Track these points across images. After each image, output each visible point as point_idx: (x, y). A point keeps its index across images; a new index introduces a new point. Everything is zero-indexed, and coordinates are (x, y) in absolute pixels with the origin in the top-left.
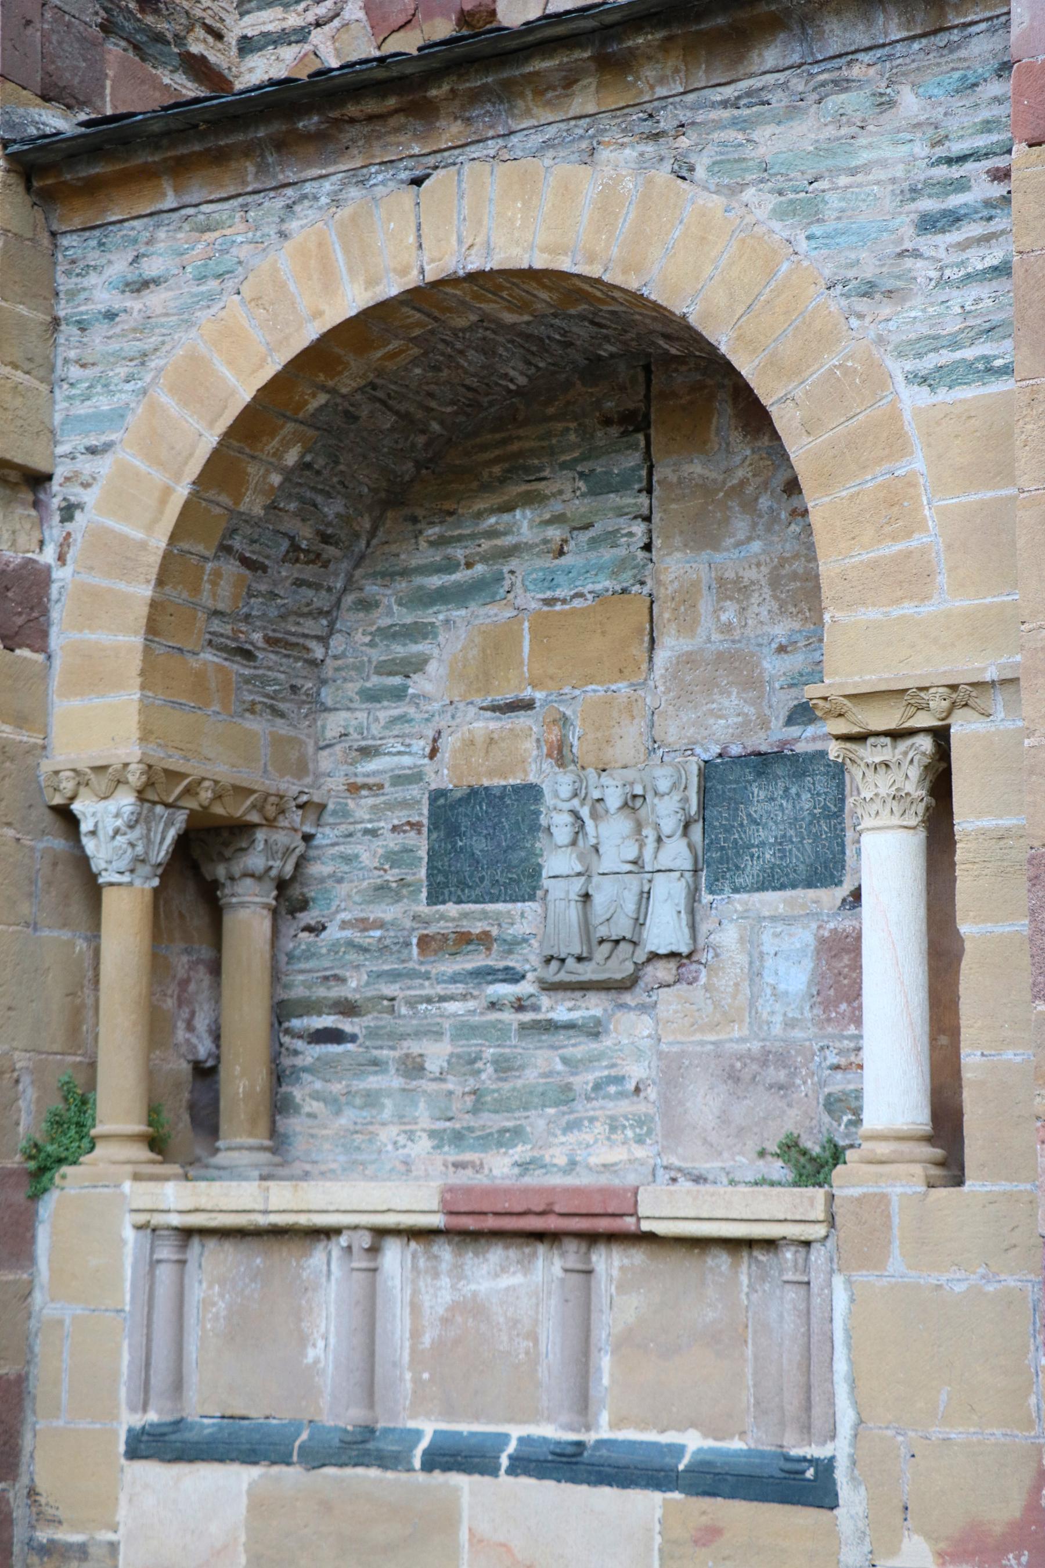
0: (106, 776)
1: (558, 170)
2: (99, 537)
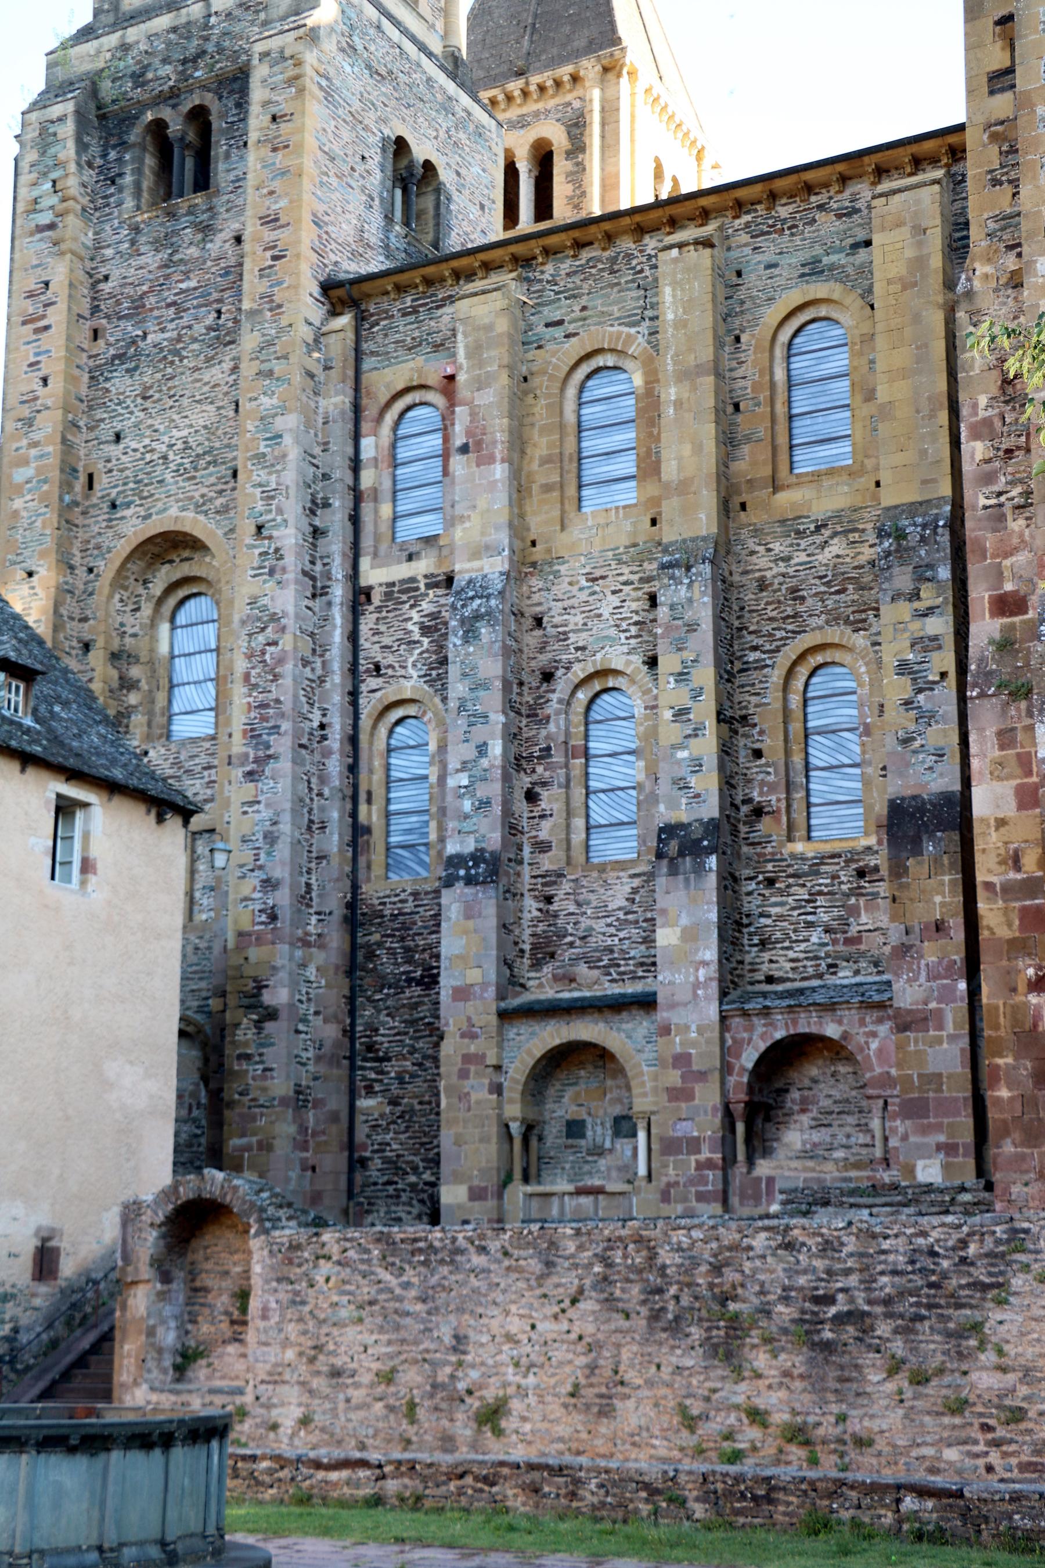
0: (514, 1119)
1: (591, 1025)
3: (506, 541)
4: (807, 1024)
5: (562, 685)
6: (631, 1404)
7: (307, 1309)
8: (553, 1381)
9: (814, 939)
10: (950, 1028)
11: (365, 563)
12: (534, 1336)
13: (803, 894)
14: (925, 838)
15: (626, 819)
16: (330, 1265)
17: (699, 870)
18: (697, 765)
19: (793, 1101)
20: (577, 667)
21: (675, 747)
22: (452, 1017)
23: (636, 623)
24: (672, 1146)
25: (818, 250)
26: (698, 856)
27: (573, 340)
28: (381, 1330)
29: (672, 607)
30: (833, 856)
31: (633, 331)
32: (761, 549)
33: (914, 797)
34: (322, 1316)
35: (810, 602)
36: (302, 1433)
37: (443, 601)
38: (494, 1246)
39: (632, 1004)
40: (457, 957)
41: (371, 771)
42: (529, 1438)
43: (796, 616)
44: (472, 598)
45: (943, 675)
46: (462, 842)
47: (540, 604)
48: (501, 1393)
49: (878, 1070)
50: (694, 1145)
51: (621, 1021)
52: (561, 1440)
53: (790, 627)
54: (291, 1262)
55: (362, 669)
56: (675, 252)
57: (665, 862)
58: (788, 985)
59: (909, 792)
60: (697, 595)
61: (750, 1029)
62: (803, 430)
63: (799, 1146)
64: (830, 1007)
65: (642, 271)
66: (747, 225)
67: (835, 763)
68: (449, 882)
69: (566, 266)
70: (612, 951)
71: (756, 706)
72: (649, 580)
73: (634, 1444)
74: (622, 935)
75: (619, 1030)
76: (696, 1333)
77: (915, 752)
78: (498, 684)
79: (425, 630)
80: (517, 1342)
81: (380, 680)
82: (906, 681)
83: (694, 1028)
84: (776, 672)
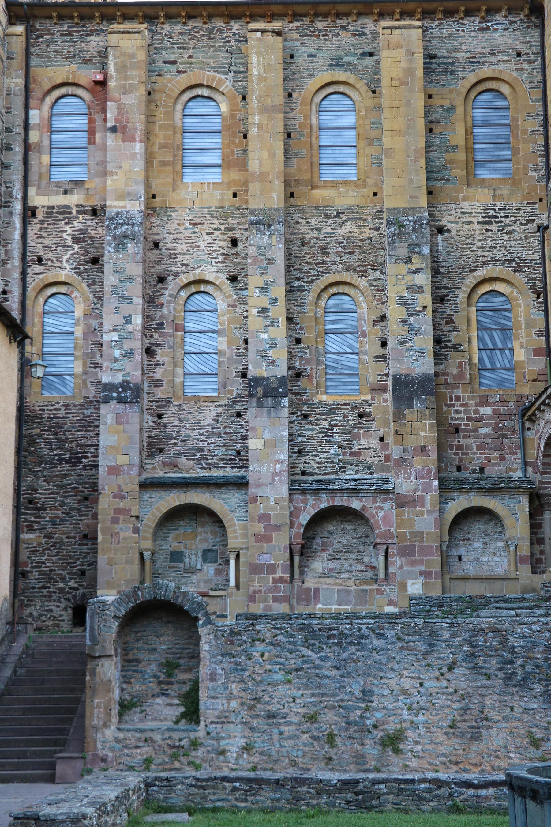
0: (147, 550)
1: (201, 495)
2: (146, 524)
3: (143, 192)
4: (340, 501)
5: (172, 286)
6: (493, 731)
7: (247, 674)
8: (437, 718)
9: (332, 451)
10: (428, 506)
11: (32, 191)
12: (423, 690)
13: (326, 425)
14: (415, 398)
15: (209, 372)
16: (264, 644)
17: (277, 406)
18: (273, 344)
19: (317, 544)
20: (182, 276)
21: (260, 331)
22: (107, 484)
23: (222, 254)
24: (256, 569)
25: (341, 52)
26: (276, 397)
27: (183, 75)
28: (306, 687)
29: (258, 248)
30: (344, 404)
31: (223, 77)
32: (303, 221)
33: (407, 375)
34: (258, 679)
35: (332, 256)
36: (245, 756)
37: (89, 223)
38: (390, 634)
39: (231, 483)
40: (111, 447)
41: (33, 325)
42: (420, 754)
43: (324, 263)
44: (122, 224)
45: (425, 307)
46: (113, 376)
47: (158, 234)
48: (399, 726)
49: (383, 529)
50: (272, 569)
51: (221, 493)
52: (444, 755)
53: (320, 269)
54: (232, 643)
55: (29, 259)
56: (259, 34)
57: (255, 399)
58: (316, 477)
59: (404, 372)
60: (274, 242)
61: (305, 502)
62: (327, 156)
63: (320, 570)
64: (355, 492)
65: (229, 42)
66: (297, 28)
67: (342, 351)
68: (106, 400)
69: (178, 28)
70: (203, 450)
71: (298, 313)
72: (232, 229)
73: (497, 757)
74: (209, 441)
75: (219, 498)
76: (538, 688)
77: (408, 349)
78: (139, 280)
79: (76, 240)
80: (409, 694)
81: (42, 267)
82: (403, 308)
83: (272, 499)
84: (311, 294)
